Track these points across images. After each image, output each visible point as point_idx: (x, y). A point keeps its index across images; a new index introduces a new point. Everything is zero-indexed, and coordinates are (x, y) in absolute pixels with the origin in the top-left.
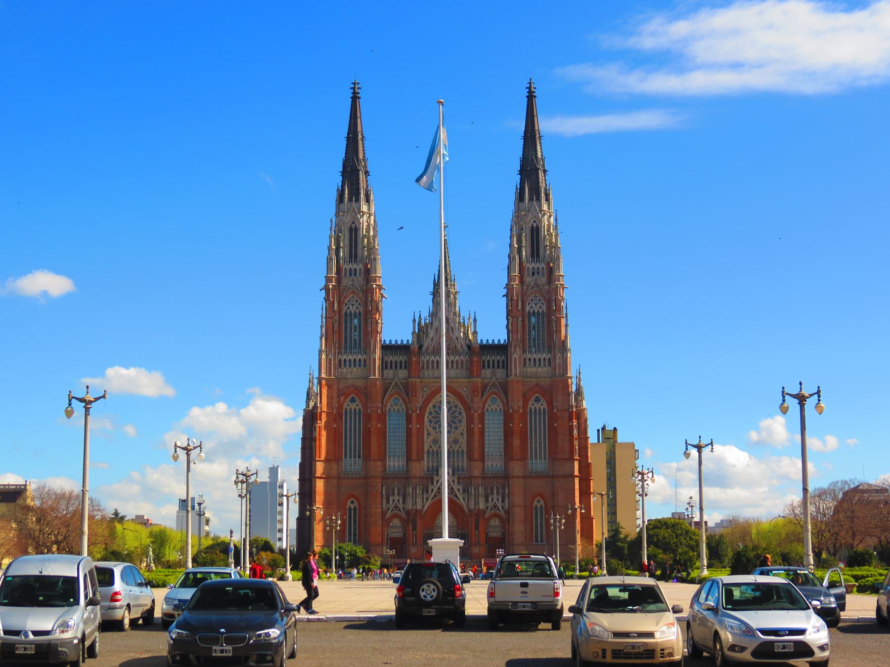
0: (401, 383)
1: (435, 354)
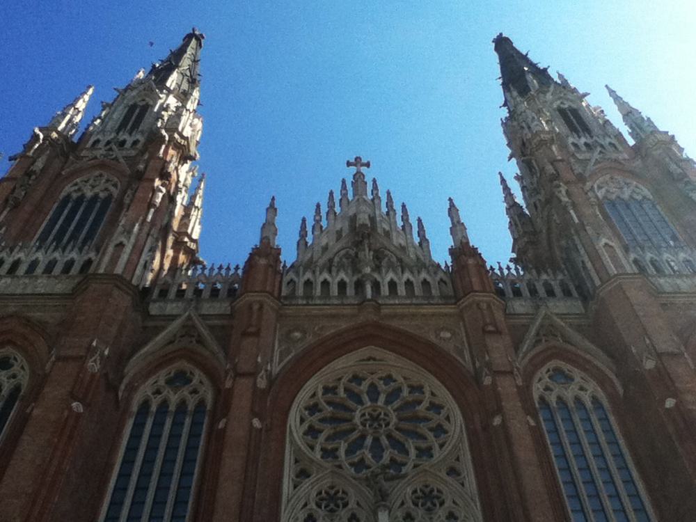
0: (212, 328)
1: (334, 269)
